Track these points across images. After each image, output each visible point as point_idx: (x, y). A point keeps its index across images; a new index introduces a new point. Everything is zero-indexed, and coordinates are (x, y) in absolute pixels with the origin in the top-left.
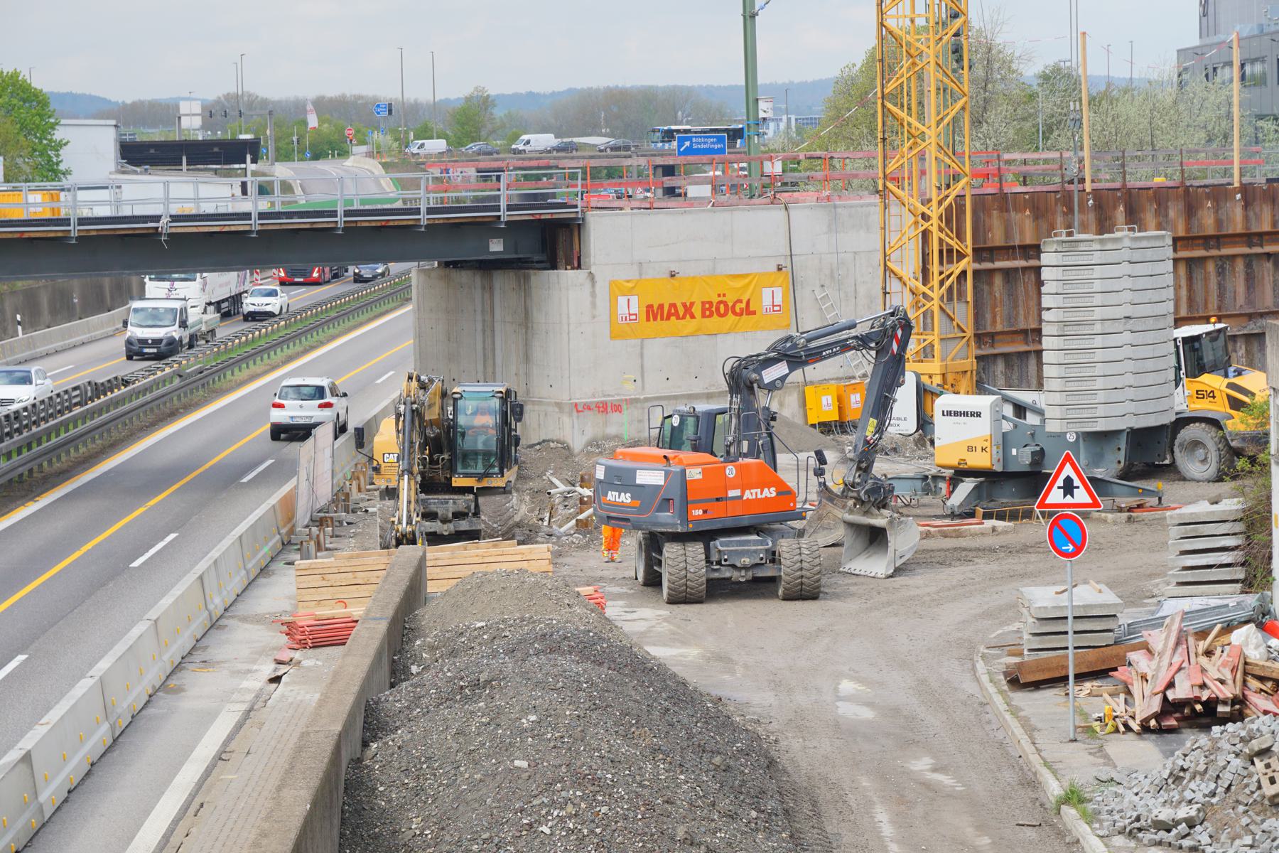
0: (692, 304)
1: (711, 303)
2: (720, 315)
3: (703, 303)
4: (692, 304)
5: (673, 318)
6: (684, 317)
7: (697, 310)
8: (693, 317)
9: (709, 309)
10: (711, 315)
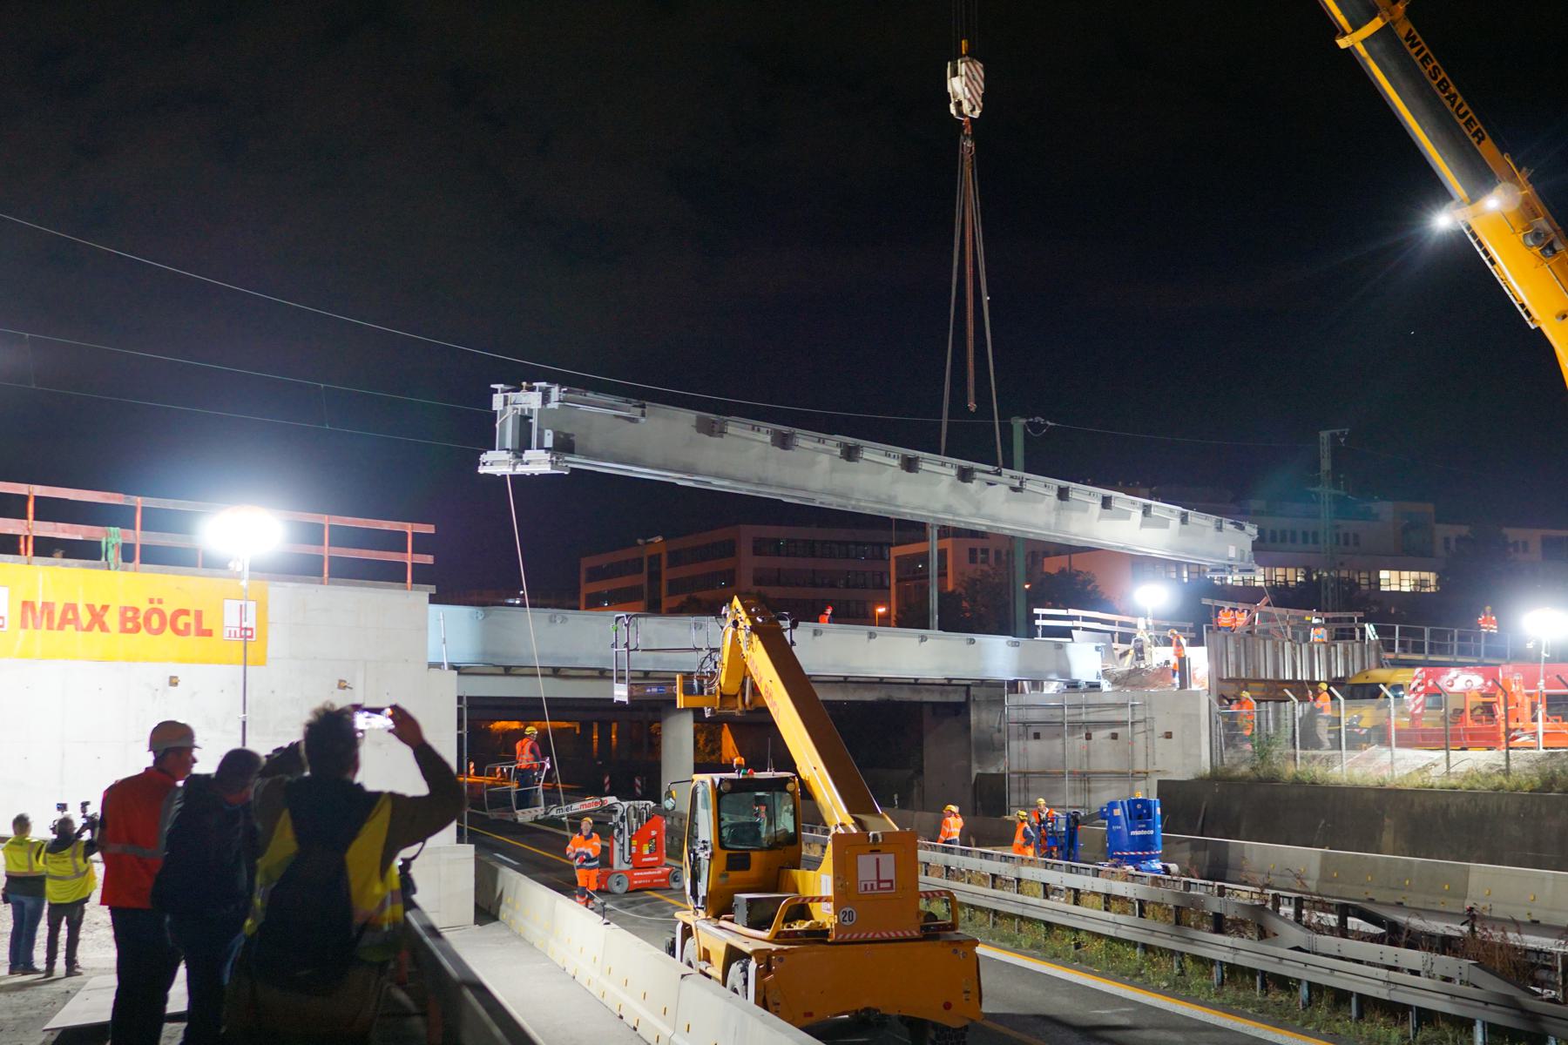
0: (105, 608)
1: (136, 610)
2: (150, 630)
3: (126, 609)
4: (105, 608)
5: (70, 628)
6: (89, 628)
7: (112, 619)
8: (104, 628)
9: (134, 619)
10: (137, 629)
